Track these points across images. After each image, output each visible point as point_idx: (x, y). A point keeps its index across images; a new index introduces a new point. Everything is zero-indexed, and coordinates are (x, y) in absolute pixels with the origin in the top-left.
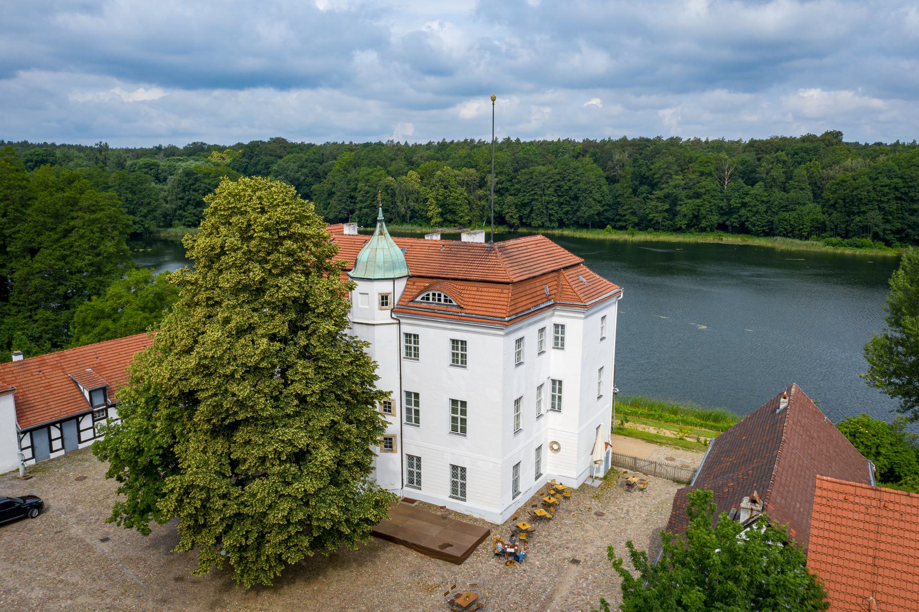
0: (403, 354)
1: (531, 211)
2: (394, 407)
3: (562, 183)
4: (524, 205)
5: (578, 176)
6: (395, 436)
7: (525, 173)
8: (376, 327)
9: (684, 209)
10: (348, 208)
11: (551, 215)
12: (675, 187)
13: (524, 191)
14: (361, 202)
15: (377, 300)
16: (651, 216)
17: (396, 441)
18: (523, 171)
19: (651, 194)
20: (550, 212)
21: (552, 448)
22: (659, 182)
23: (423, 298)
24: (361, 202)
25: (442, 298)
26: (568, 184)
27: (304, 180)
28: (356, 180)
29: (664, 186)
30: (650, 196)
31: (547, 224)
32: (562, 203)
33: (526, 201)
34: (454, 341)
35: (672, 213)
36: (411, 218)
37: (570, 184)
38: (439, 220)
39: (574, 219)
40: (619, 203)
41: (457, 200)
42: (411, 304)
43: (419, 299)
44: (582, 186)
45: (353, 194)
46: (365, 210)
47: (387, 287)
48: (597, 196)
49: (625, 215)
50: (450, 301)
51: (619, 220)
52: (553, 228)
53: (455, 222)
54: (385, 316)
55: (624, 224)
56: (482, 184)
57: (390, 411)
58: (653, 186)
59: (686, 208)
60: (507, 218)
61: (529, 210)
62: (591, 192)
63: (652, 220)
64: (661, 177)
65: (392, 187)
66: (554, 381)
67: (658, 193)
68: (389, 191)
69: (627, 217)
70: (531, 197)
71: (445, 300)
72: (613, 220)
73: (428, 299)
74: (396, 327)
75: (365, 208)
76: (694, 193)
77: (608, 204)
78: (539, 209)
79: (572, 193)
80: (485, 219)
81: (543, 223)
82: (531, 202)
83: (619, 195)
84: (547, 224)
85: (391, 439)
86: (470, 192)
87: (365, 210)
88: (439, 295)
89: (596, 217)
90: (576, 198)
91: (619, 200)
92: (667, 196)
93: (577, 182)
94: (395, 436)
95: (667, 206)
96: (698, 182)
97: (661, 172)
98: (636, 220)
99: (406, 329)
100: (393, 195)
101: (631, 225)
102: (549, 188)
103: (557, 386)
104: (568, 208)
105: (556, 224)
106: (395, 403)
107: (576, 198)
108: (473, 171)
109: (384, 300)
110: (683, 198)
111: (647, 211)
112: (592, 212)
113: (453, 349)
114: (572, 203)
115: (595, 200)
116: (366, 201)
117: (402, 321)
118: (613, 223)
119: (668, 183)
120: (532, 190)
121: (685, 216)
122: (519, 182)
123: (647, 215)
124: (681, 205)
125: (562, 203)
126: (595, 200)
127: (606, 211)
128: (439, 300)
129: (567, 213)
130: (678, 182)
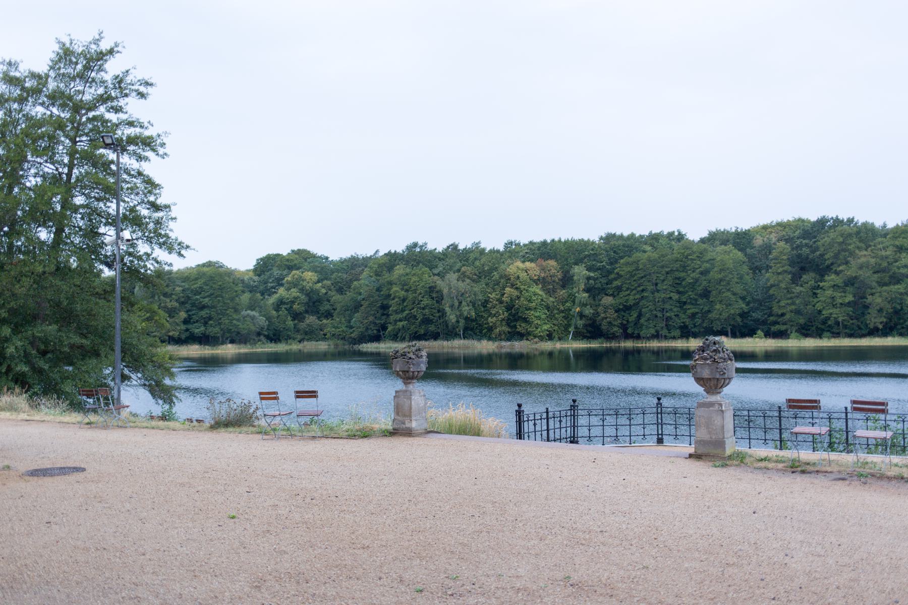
1: (640, 316)
3: (682, 275)
4: (627, 308)
5: (707, 262)
7: (627, 264)
9: (879, 300)
10: (378, 322)
11: (668, 319)
13: (628, 289)
14: (396, 312)
16: (825, 313)
18: (622, 261)
20: (668, 314)
22: (832, 264)
24: (396, 312)
26: (693, 275)
27: (326, 293)
28: (391, 283)
29: (841, 268)
30: (821, 284)
31: (664, 332)
32: (685, 303)
33: (631, 303)
35: (860, 307)
36: (466, 329)
37: (695, 275)
38: (506, 329)
39: (705, 325)
40: (771, 297)
41: (529, 301)
44: (714, 275)
45: (385, 302)
46: (400, 324)
48: (738, 289)
49: (783, 315)
51: (775, 323)
52: (674, 338)
53: (529, 334)
55: (783, 328)
56: (567, 280)
58: (822, 270)
59: (877, 300)
60: (604, 327)
61: (635, 315)
62: (728, 284)
63: (828, 318)
64: (836, 256)
65: (438, 288)
67: (831, 278)
68: (434, 295)
69: (787, 317)
70: (638, 296)
72: (764, 322)
75: (400, 320)
76: (891, 277)
77: (755, 301)
78: (651, 311)
79: (699, 289)
80: (572, 329)
81: (657, 331)
82: (638, 303)
83: (772, 286)
84: (664, 332)
86: (549, 292)
87: (400, 324)
89: (739, 319)
90: (706, 294)
91: (771, 292)
92: (851, 282)
93: (705, 273)
95: (850, 298)
96: (896, 261)
97: (836, 248)
98: (802, 321)
100: (440, 299)
101: (794, 329)
102: (663, 281)
104: (692, 310)
105: (677, 333)
107: (706, 294)
108: (552, 263)
111: (819, 306)
112: (732, 312)
114: (700, 301)
115: (734, 294)
116: (403, 311)
118: (765, 328)
119: (847, 263)
120: (639, 286)
121: (880, 310)
122: (619, 276)
123: (820, 312)
124: (872, 294)
125: (685, 303)
126: (734, 294)
127: (753, 310)
129: (693, 316)
130: (863, 260)
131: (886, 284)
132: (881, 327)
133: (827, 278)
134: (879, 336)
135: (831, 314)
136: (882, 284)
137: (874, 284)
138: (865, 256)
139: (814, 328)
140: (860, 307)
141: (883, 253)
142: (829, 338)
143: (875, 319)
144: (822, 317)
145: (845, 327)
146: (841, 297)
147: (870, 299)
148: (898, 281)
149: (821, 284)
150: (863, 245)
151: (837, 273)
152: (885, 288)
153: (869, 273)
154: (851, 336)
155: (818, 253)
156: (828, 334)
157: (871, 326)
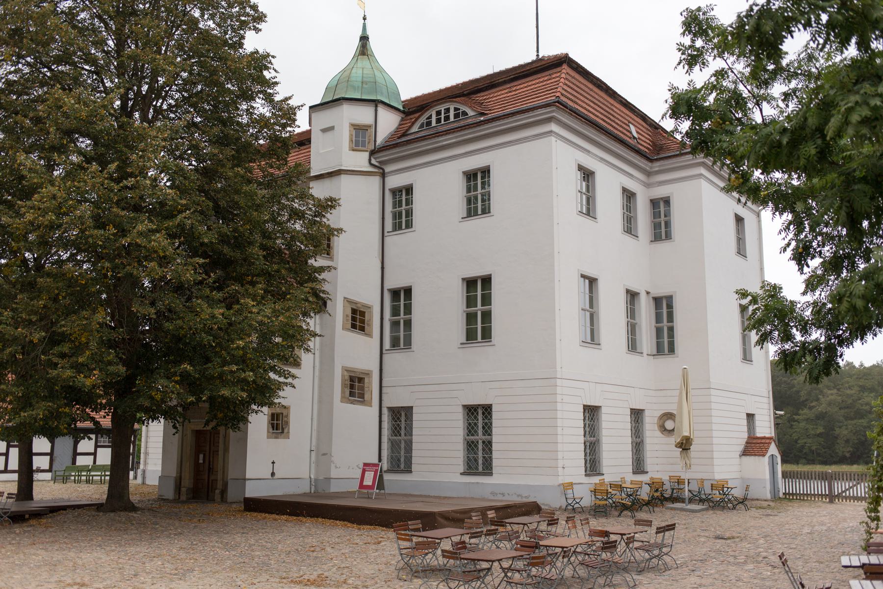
0: (389, 226)
2: (371, 320)
6: (368, 374)
8: (343, 177)
9: (845, 432)
12: (830, 404)
15: (345, 134)
16: (801, 442)
17: (370, 383)
19: (797, 414)
21: (663, 429)
23: (422, 126)
25: (452, 114)
30: (796, 417)
34: (470, 176)
35: (829, 437)
42: (404, 139)
43: (415, 129)
47: (363, 115)
50: (465, 113)
54: (360, 160)
57: (362, 329)
59: (843, 432)
63: (803, 447)
66: (657, 301)
71: (456, 116)
73: (429, 124)
74: (376, 181)
85: (361, 380)
88: (448, 110)
94: (368, 374)
95: (820, 430)
99: (395, 181)
103: (665, 310)
106: (371, 313)
109: (359, 130)
110: (841, 418)
111: (795, 436)
113: (469, 190)
117: (388, 169)
119: (818, 400)
121: (847, 441)
128: (447, 118)
131: (852, 419)
132: (848, 455)
133: (801, 412)
134: (848, 464)
135: (805, 443)
136: (847, 418)
137: (841, 418)
138: (832, 394)
139: (791, 456)
140: (829, 437)
141: (849, 392)
142: (804, 464)
143: (842, 449)
144: (798, 445)
145: (819, 455)
146: (813, 429)
147: (837, 431)
148: (862, 417)
149: (796, 417)
150: (832, 385)
151: (811, 408)
152: (850, 422)
153: (836, 409)
154: (825, 463)
155: (794, 389)
156: (804, 461)
157: (840, 454)
